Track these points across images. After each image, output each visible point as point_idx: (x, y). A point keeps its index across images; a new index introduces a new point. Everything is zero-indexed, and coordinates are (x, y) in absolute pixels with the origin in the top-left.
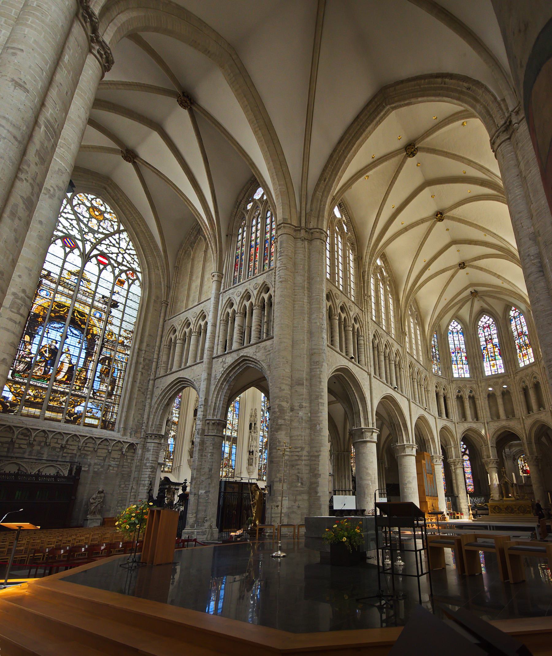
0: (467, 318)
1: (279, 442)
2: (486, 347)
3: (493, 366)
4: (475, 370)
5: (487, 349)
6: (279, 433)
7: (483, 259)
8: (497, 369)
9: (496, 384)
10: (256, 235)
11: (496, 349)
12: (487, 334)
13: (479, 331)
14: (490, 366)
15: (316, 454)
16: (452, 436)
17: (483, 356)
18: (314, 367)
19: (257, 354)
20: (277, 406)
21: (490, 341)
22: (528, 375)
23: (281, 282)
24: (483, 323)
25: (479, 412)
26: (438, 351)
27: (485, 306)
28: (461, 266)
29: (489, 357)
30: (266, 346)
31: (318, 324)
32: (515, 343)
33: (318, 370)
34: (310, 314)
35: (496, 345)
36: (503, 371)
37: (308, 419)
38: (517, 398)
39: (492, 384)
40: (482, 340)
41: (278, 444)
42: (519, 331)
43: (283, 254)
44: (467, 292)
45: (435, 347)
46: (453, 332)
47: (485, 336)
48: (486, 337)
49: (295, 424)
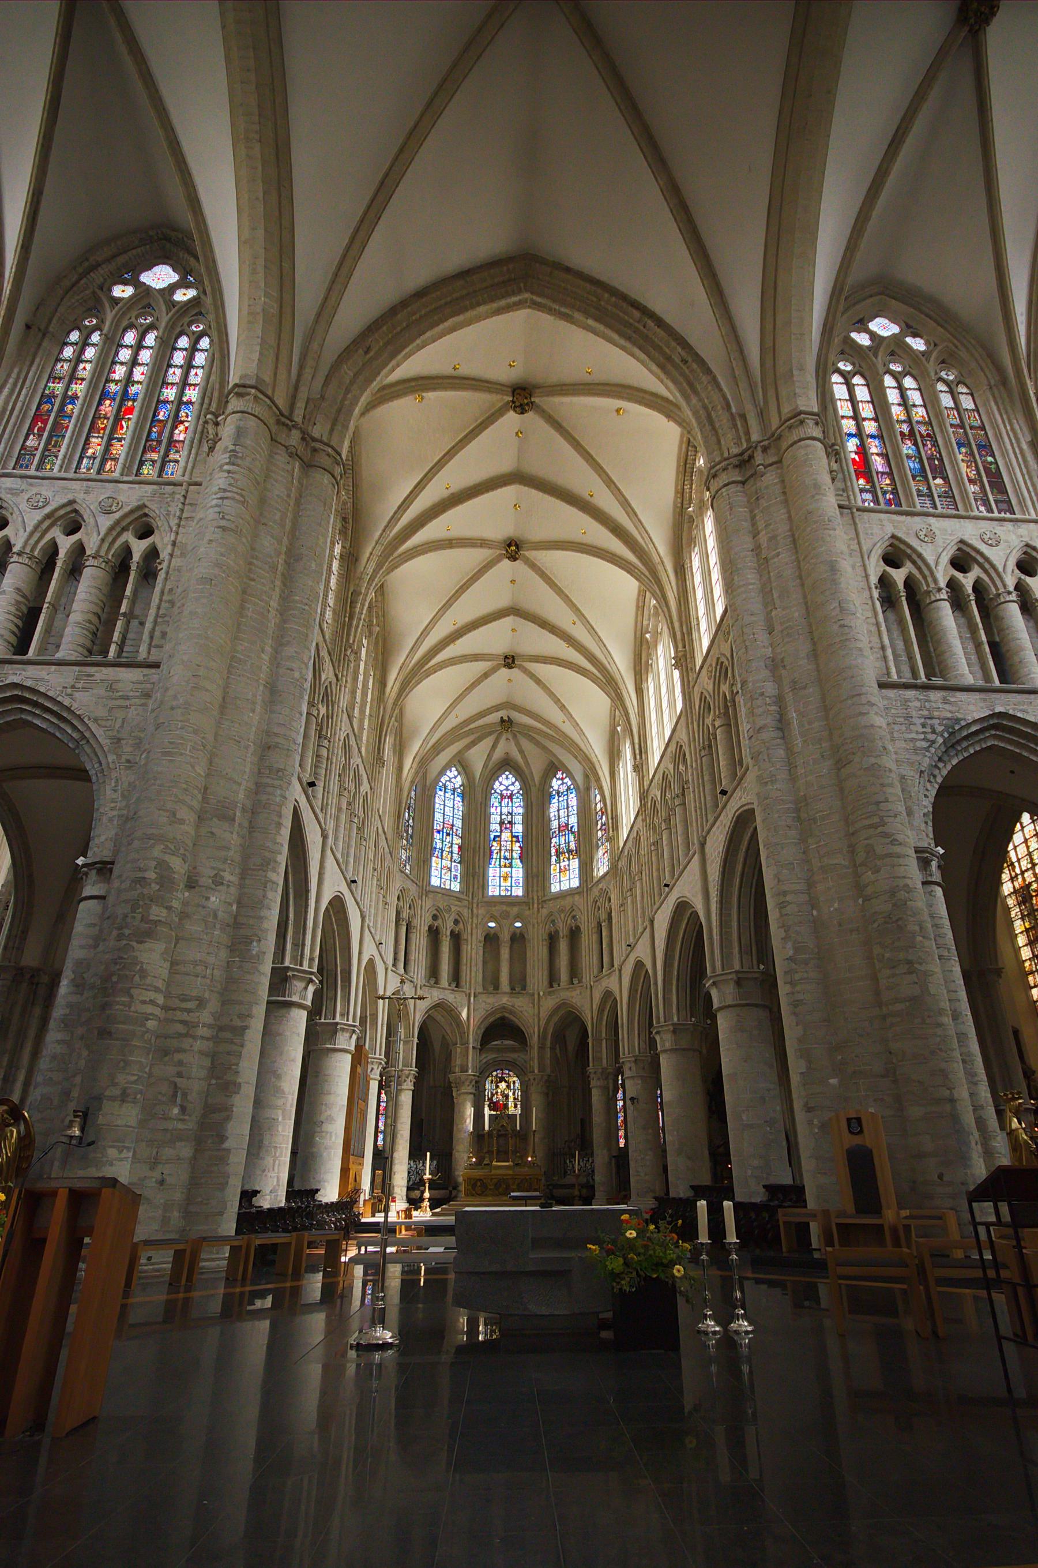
0: (478, 768)
1: (143, 973)
3: (505, 879)
4: (471, 878)
5: (500, 841)
6: (147, 945)
7: (551, 664)
8: (511, 886)
9: (506, 915)
11: (516, 847)
12: (505, 810)
13: (493, 800)
14: (500, 877)
15: (239, 1024)
17: (491, 852)
18: (268, 781)
20: (153, 864)
21: (508, 826)
22: (563, 911)
24: (502, 788)
26: (413, 819)
28: (507, 660)
29: (500, 859)
31: (297, 675)
35: (517, 837)
36: (520, 893)
37: (231, 921)
38: (536, 953)
40: (495, 819)
41: (137, 978)
42: (563, 820)
45: (409, 810)
46: (445, 787)
47: (501, 815)
48: (503, 817)
49: (194, 927)
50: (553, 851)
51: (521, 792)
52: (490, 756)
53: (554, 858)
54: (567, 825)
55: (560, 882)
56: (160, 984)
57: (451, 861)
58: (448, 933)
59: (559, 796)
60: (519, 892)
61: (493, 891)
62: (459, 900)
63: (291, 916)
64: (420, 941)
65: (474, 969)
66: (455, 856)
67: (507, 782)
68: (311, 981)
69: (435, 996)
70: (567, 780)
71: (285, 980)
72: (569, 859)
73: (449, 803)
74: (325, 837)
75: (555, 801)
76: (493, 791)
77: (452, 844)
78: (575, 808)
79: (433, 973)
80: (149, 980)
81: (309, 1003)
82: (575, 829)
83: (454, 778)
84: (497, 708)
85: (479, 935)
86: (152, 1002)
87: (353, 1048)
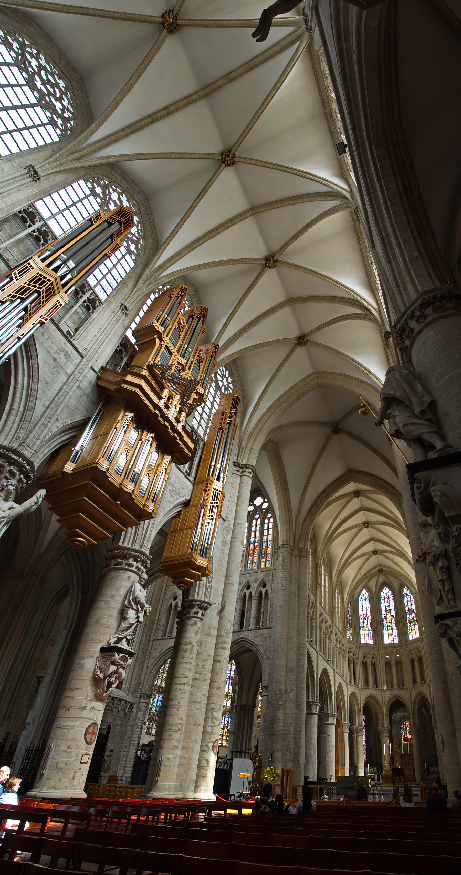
0: (373, 588)
1: (279, 719)
10: (255, 535)
12: (387, 605)
16: (357, 702)
17: (383, 624)
19: (255, 639)
23: (283, 590)
25: (378, 679)
34: (299, 616)
39: (389, 652)
40: (383, 609)
43: (284, 568)
44: (376, 569)
52: (377, 584)
56: (282, 721)
58: (370, 664)
61: (386, 642)
62: (373, 648)
63: (310, 683)
64: (360, 669)
65: (382, 679)
66: (370, 628)
67: (386, 592)
68: (318, 705)
69: (368, 692)
71: (310, 705)
74: (317, 653)
79: (366, 682)
80: (280, 720)
81: (318, 712)
84: (375, 567)
85: (383, 663)
86: (281, 726)
87: (335, 723)
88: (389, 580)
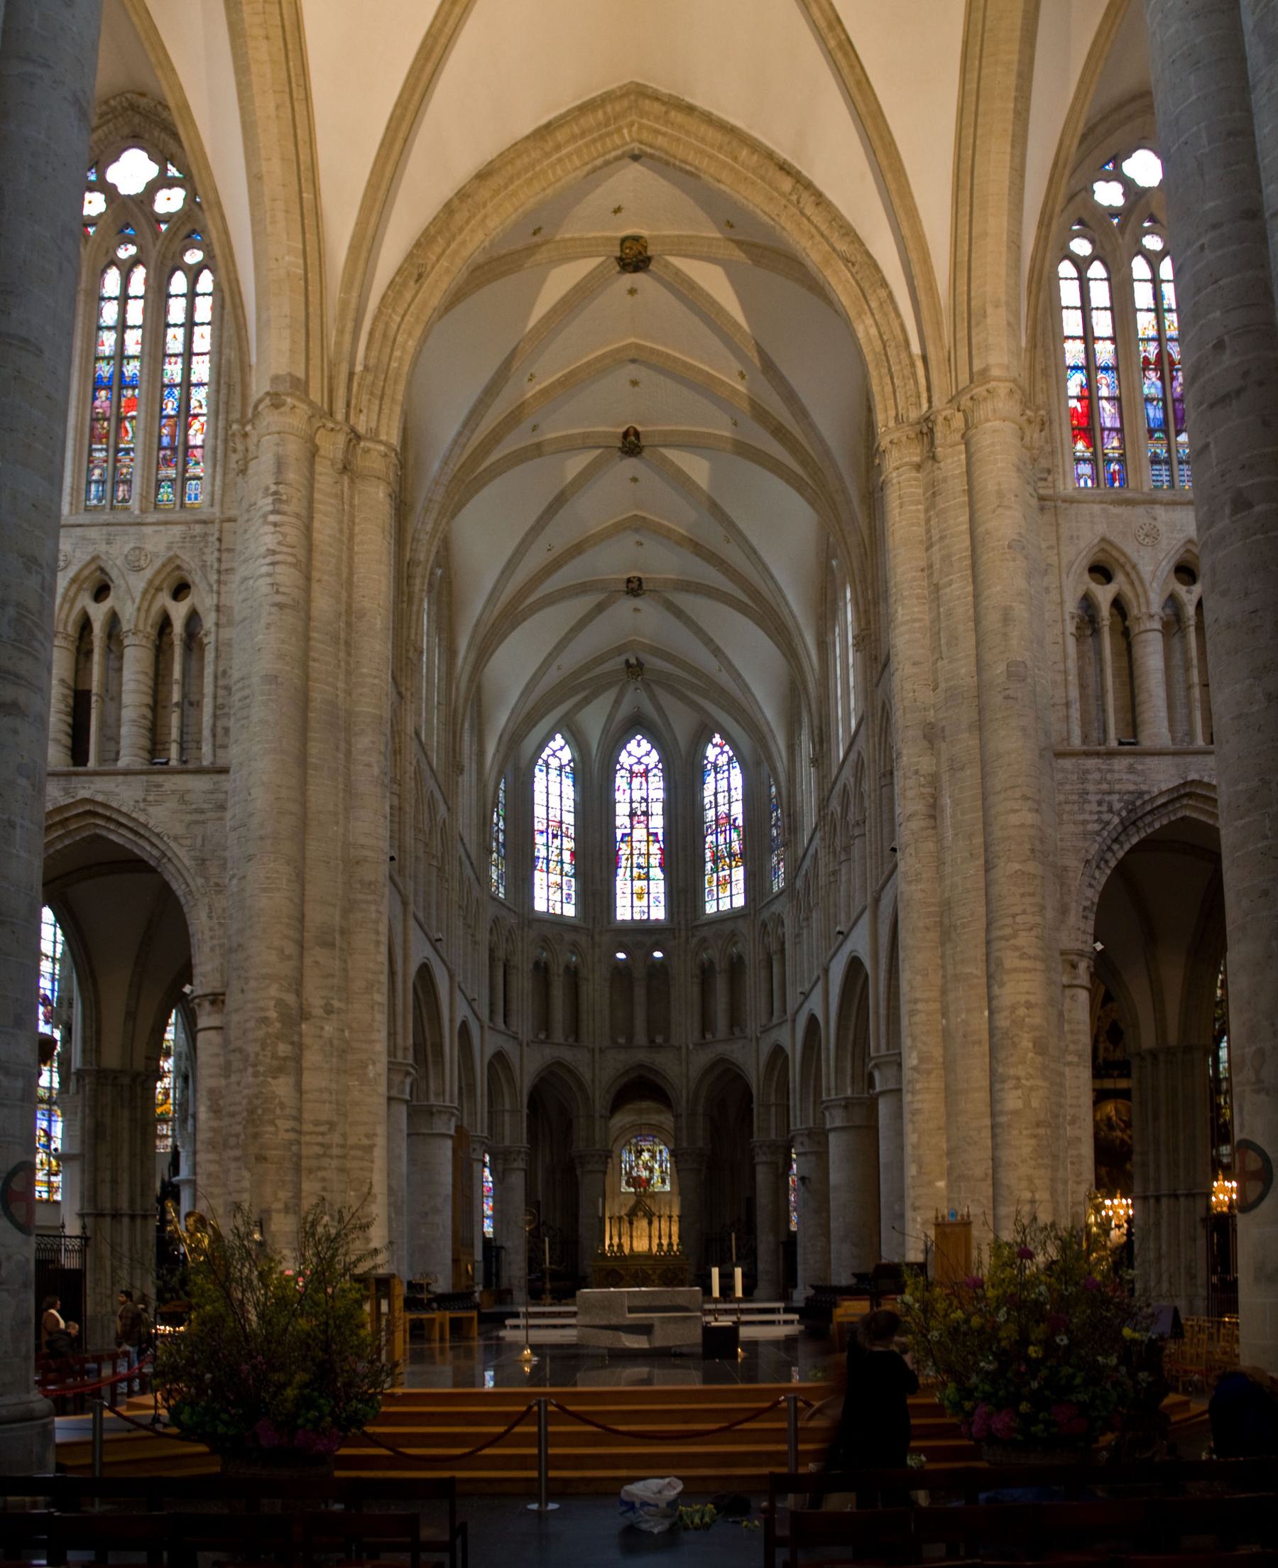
0: (594, 738)
2: (630, 835)
3: (640, 896)
11: (655, 848)
12: (637, 796)
21: (642, 818)
26: (504, 819)
27: (649, 709)
29: (632, 867)
30: (188, 791)
32: (705, 842)
33: (373, 908)
35: (656, 834)
40: (622, 809)
47: (631, 802)
50: (708, 854)
51: (660, 766)
53: (709, 866)
54: (728, 816)
55: (718, 899)
57: (561, 875)
59: (716, 773)
60: (658, 913)
61: (623, 913)
66: (567, 868)
67: (639, 751)
70: (727, 748)
72: (730, 868)
73: (554, 789)
75: (710, 780)
76: (618, 767)
77: (562, 849)
78: (740, 790)
82: (740, 822)
83: (559, 751)
88: (659, 709)
